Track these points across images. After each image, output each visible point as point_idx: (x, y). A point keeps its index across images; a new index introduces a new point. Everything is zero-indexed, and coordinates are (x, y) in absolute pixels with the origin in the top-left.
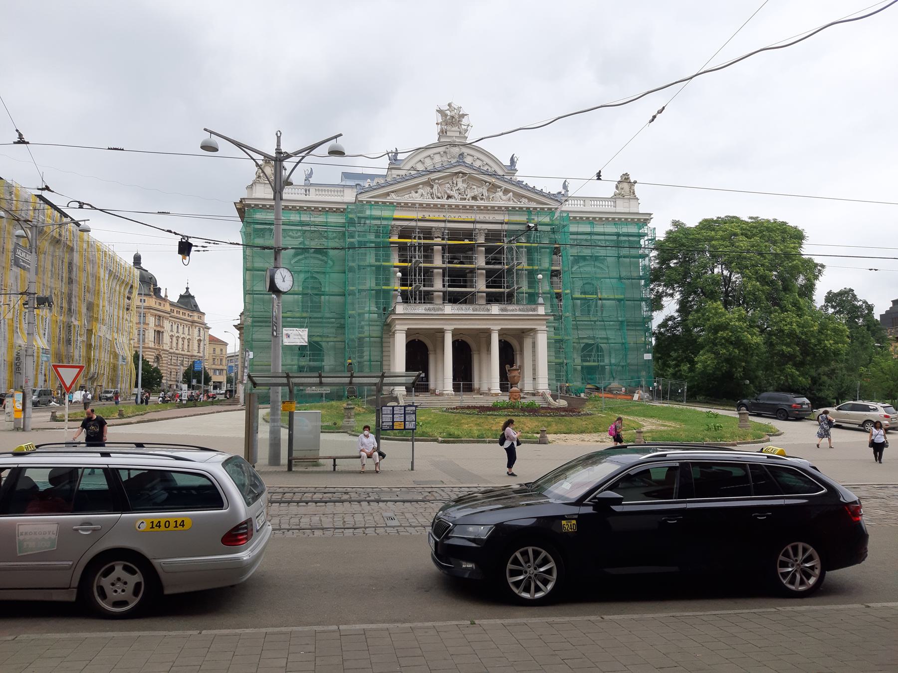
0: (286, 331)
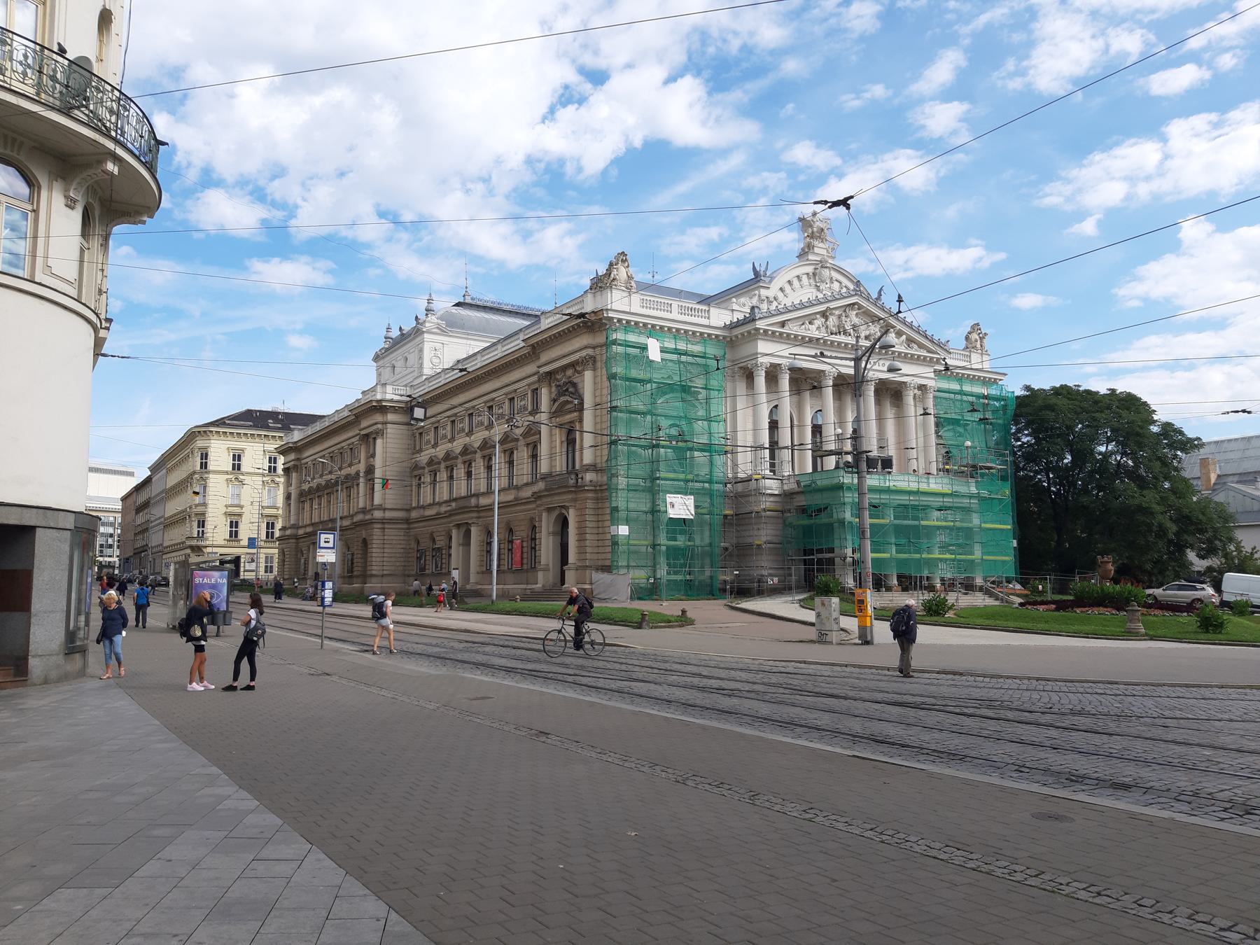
0: (670, 498)
